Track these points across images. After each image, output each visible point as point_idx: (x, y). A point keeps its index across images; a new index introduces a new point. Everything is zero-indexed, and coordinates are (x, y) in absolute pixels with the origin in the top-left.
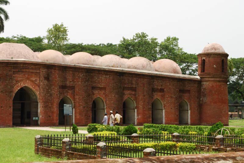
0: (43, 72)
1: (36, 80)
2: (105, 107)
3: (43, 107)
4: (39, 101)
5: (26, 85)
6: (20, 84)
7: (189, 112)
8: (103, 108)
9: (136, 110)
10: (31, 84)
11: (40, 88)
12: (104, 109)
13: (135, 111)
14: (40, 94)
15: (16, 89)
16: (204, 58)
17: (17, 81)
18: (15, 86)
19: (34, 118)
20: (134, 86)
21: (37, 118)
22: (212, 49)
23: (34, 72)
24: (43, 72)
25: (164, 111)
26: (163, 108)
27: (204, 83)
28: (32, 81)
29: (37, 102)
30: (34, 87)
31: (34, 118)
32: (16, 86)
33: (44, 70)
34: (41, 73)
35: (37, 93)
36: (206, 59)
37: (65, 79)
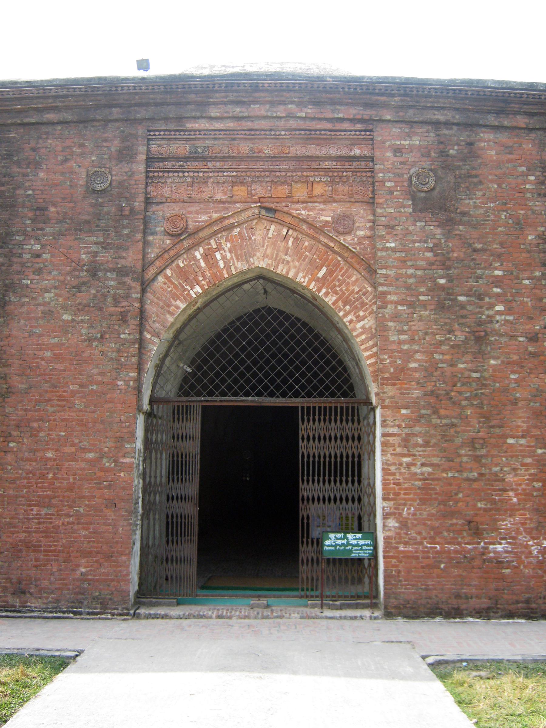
0: (398, 151)
1: (343, 224)
3: (406, 441)
5: (261, 262)
6: (208, 256)
10: (299, 254)
11: (374, 286)
17: (184, 236)
18: (160, 272)
19: (333, 541)
21: (354, 543)
24: (398, 151)
30: (330, 272)
31: (333, 541)
32: (168, 272)
33: (409, 136)
34: (387, 159)
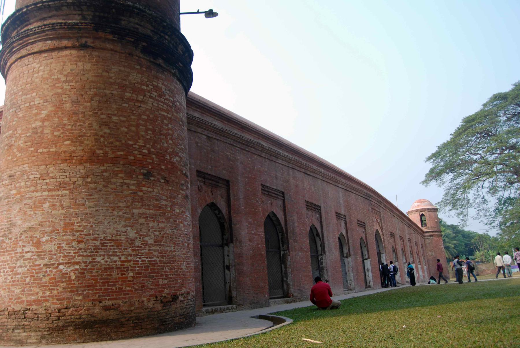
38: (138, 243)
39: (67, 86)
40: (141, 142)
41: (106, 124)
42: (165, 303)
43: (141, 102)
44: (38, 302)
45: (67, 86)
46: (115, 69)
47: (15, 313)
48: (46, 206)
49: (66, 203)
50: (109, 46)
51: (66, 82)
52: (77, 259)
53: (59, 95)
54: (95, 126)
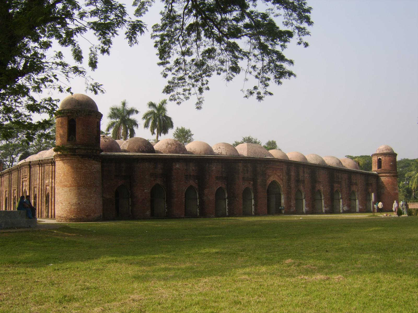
2: (323, 198)
4: (282, 193)
5: (275, 179)
7: (304, 201)
8: (355, 199)
9: (341, 200)
12: (321, 199)
13: (340, 201)
14: (283, 187)
15: (269, 182)
16: (380, 157)
17: (269, 176)
20: (340, 180)
22: (386, 150)
23: (279, 168)
24: (285, 168)
25: (357, 201)
26: (356, 199)
27: (381, 178)
28: (278, 176)
29: (280, 194)
35: (282, 186)
36: (382, 158)
37: (298, 175)
38: (81, 204)
39: (65, 169)
40: (81, 181)
41: (73, 178)
42: (87, 216)
43: (81, 171)
44: (63, 215)
45: (65, 169)
46: (75, 164)
47: (59, 216)
48: (63, 196)
49: (66, 195)
50: (73, 159)
51: (65, 168)
52: (69, 207)
53: (64, 171)
54: (71, 179)
